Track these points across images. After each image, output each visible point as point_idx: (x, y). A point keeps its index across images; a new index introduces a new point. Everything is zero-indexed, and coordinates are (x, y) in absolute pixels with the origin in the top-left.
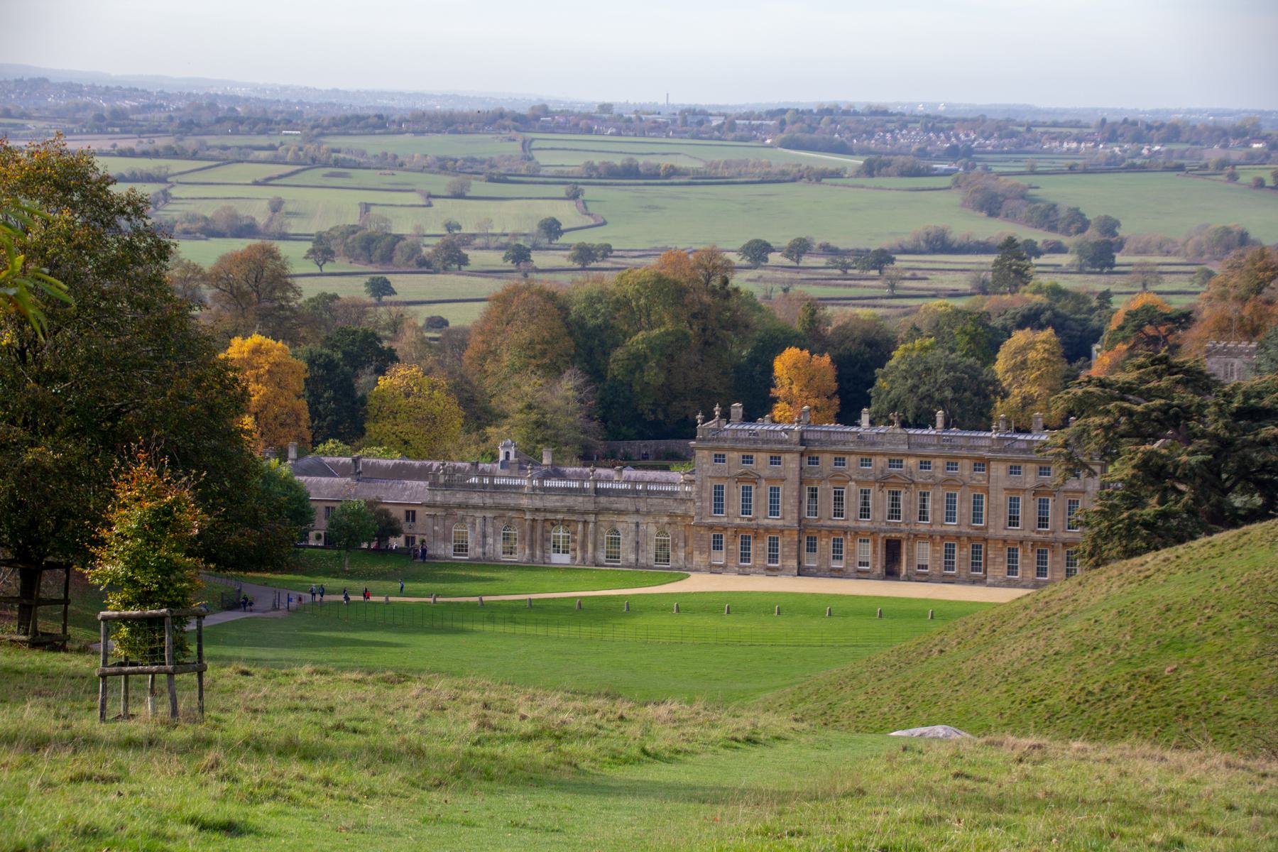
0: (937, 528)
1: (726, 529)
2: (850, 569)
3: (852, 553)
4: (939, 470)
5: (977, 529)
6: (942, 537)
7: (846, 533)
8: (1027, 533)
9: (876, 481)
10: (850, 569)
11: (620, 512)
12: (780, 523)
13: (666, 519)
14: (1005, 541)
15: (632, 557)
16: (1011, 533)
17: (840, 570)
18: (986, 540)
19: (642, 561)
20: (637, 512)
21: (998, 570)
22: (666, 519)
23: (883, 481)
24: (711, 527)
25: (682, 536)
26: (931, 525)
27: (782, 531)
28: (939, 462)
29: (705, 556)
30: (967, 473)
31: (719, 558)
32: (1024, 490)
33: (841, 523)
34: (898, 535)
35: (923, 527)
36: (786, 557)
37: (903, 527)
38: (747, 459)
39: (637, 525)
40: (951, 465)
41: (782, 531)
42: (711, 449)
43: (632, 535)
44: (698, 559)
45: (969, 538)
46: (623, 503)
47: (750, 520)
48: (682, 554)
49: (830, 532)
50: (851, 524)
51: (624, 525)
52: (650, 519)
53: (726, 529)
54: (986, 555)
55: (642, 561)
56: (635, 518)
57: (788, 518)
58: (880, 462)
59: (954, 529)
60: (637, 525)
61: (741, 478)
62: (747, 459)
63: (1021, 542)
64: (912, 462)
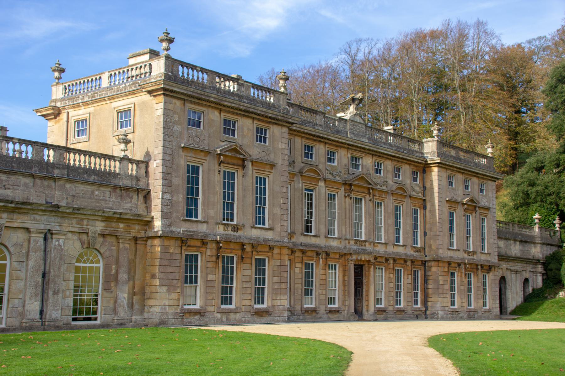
0: (390, 249)
1: (204, 243)
2: (322, 310)
3: (324, 284)
4: (390, 176)
5: (418, 250)
6: (394, 260)
7: (318, 254)
8: (461, 255)
9: (345, 184)
10: (323, 307)
11: (19, 207)
12: (269, 235)
13: (99, 226)
14: (449, 264)
15: (34, 306)
16: (450, 254)
17: (314, 311)
18: (424, 263)
19: (53, 313)
20: (54, 209)
21: (438, 302)
22: (99, 226)
23: (348, 185)
24: (183, 241)
25: (124, 260)
26: (386, 244)
27: (271, 248)
28: (388, 165)
29: (174, 296)
30: (408, 182)
31: (197, 297)
32: (457, 203)
33: (313, 241)
34: (367, 257)
35: (381, 249)
36: (276, 292)
37: (369, 247)
38: (229, 128)
39: (47, 235)
40: (397, 172)
41: (271, 248)
42: (185, 98)
43: (35, 258)
44: (162, 302)
45: (412, 262)
46: (20, 189)
47: (236, 229)
48: (123, 296)
49: (303, 252)
50: (321, 242)
51: (20, 236)
52: (71, 225)
53: (204, 243)
54: (426, 281)
55: (53, 313)
56: (39, 223)
57: (278, 228)
58: (342, 157)
59: (401, 250)
60: (47, 235)
61: (221, 159)
62: (229, 128)
63: (459, 265)
64: (368, 162)
